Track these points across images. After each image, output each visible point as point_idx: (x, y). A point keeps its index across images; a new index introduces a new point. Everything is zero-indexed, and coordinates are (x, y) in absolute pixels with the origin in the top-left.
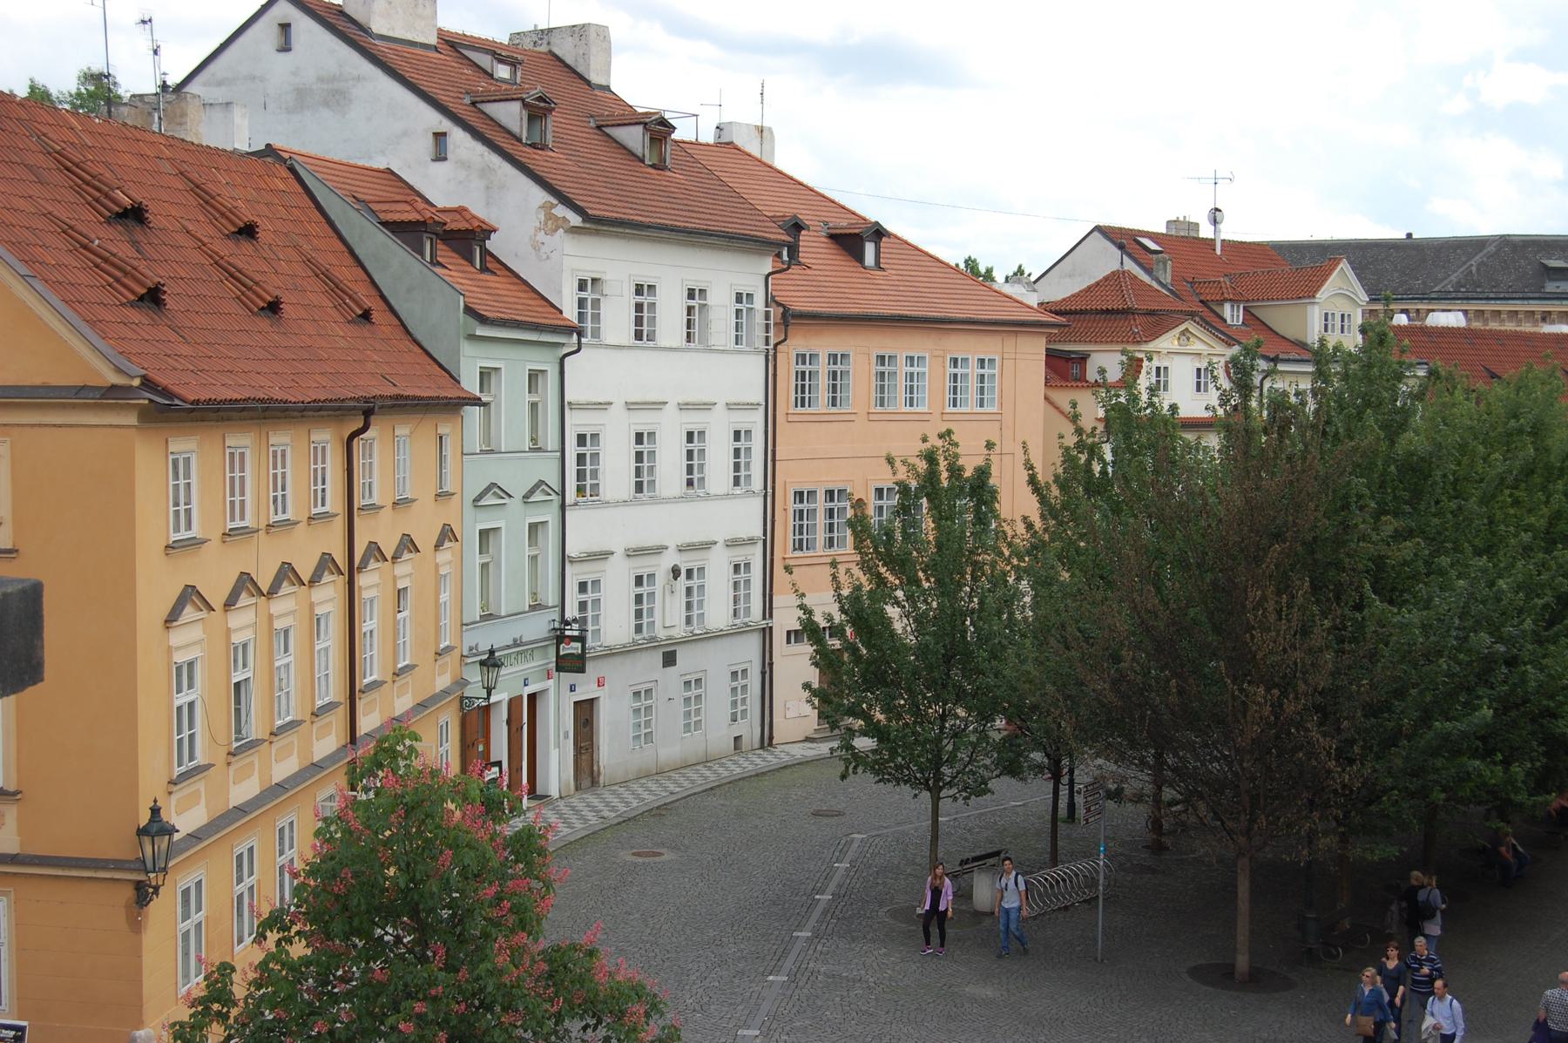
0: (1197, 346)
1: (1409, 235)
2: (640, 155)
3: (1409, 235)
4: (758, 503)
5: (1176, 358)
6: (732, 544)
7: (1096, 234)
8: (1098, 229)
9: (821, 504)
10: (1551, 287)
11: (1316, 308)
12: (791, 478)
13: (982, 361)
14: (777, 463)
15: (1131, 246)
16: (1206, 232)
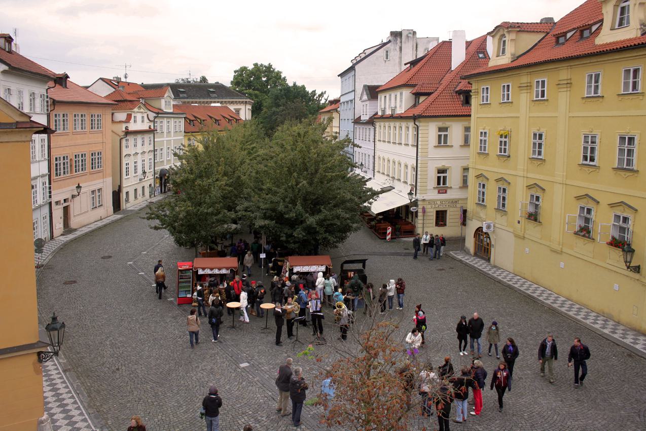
0: (142, 110)
1: (142, 83)
2: (3, 47)
3: (142, 83)
4: (46, 163)
5: (138, 113)
6: (43, 176)
7: (100, 80)
8: (101, 79)
9: (62, 161)
10: (181, 95)
11: (164, 100)
12: (54, 154)
13: (82, 115)
14: (51, 150)
15: (110, 83)
16: (123, 80)
